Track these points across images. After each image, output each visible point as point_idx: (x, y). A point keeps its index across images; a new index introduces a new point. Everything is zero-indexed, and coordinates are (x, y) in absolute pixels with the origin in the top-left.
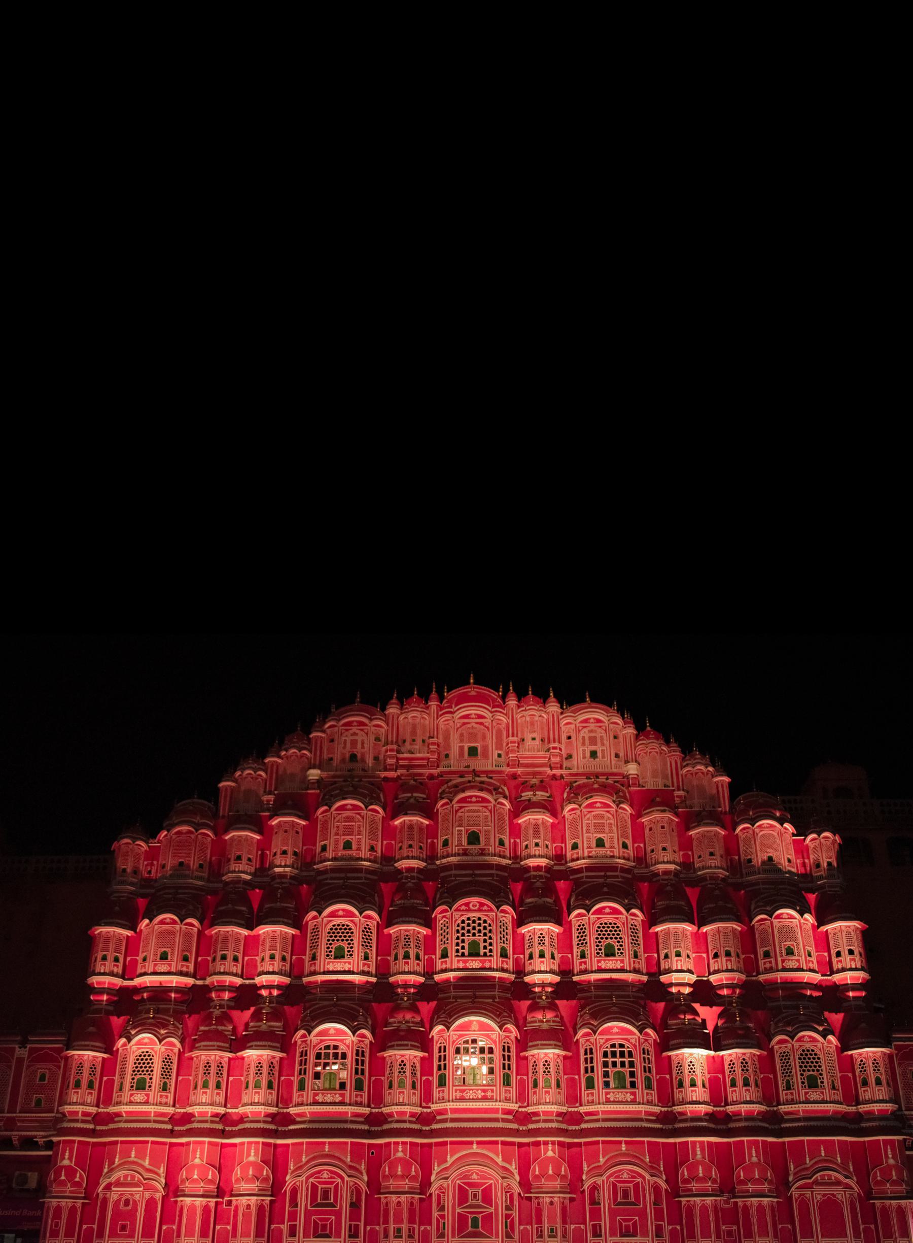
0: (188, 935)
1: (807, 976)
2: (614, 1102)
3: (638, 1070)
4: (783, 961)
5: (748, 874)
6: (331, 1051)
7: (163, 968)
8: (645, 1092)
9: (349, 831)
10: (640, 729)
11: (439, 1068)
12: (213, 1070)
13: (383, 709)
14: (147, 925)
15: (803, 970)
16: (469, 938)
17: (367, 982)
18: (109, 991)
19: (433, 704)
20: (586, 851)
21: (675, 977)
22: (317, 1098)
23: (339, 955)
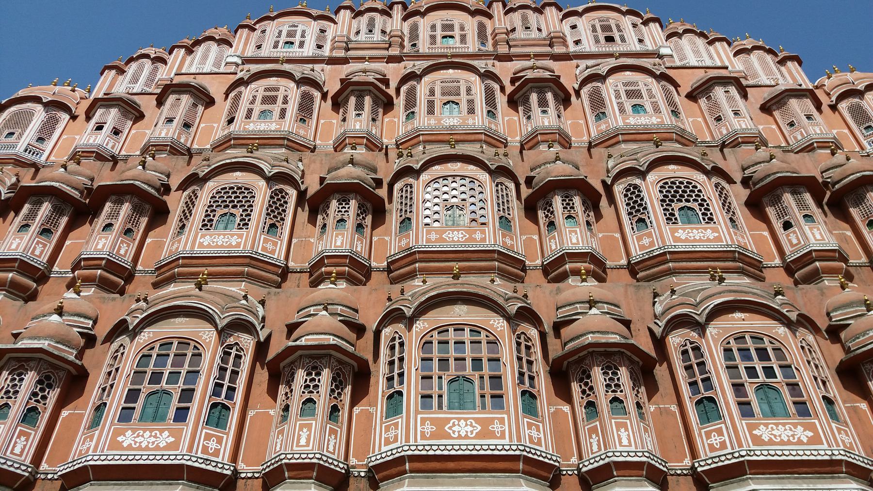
2: (771, 442)
8: (833, 425)
11: (390, 379)
20: (619, 119)
22: (120, 439)
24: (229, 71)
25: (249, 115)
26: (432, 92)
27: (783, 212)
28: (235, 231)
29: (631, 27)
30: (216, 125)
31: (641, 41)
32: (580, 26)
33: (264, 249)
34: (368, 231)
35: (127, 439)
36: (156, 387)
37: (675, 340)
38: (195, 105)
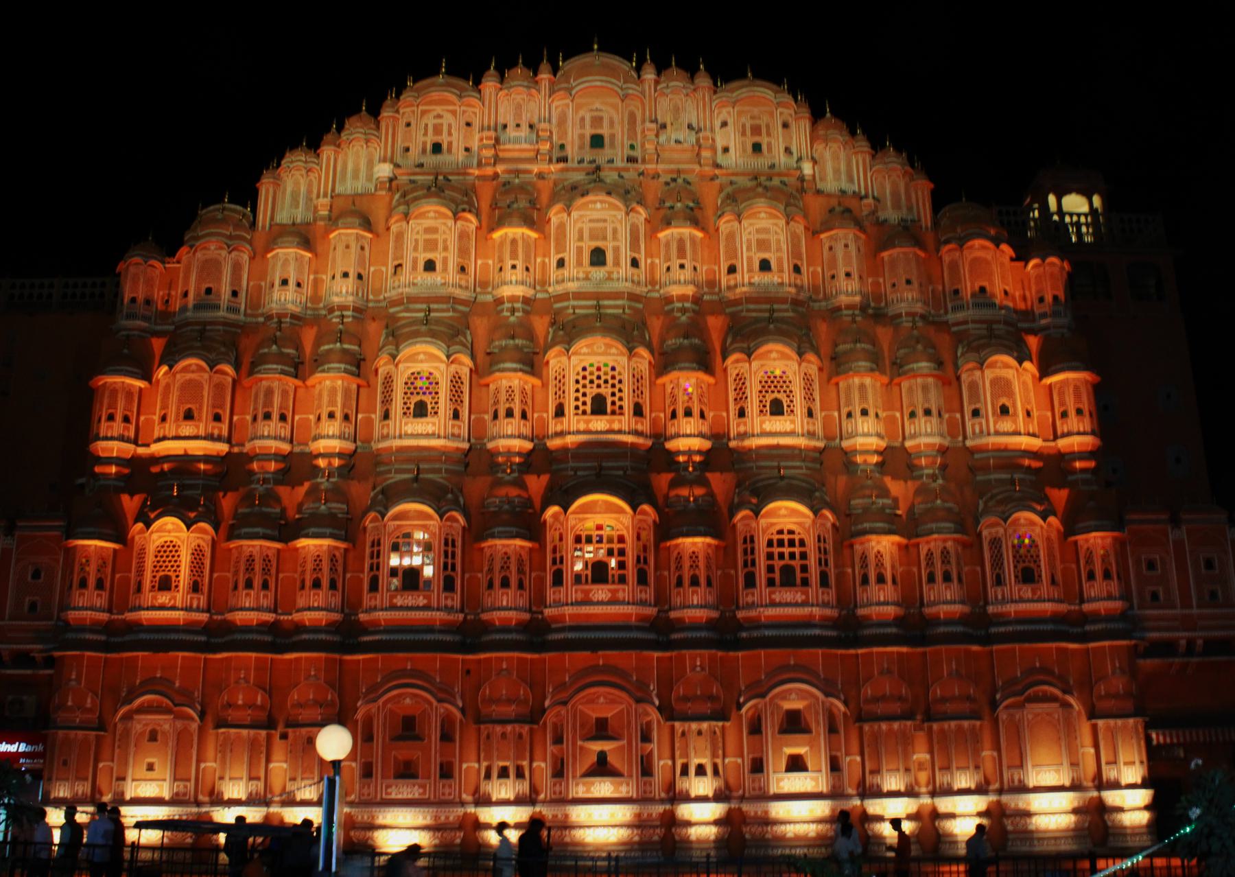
0: (219, 388)
1: (1024, 442)
3: (812, 562)
4: (995, 423)
5: (954, 309)
7: (188, 429)
9: (431, 245)
10: (817, 116)
12: (258, 567)
13: (477, 83)
14: (165, 374)
15: (1020, 434)
16: (592, 391)
17: (457, 449)
18: (118, 461)
19: (545, 76)
21: (860, 441)
23: (421, 411)
25: (414, 268)
26: (581, 238)
27: (849, 403)
28: (429, 419)
30: (384, 269)
32: (730, 121)
38: (362, 248)
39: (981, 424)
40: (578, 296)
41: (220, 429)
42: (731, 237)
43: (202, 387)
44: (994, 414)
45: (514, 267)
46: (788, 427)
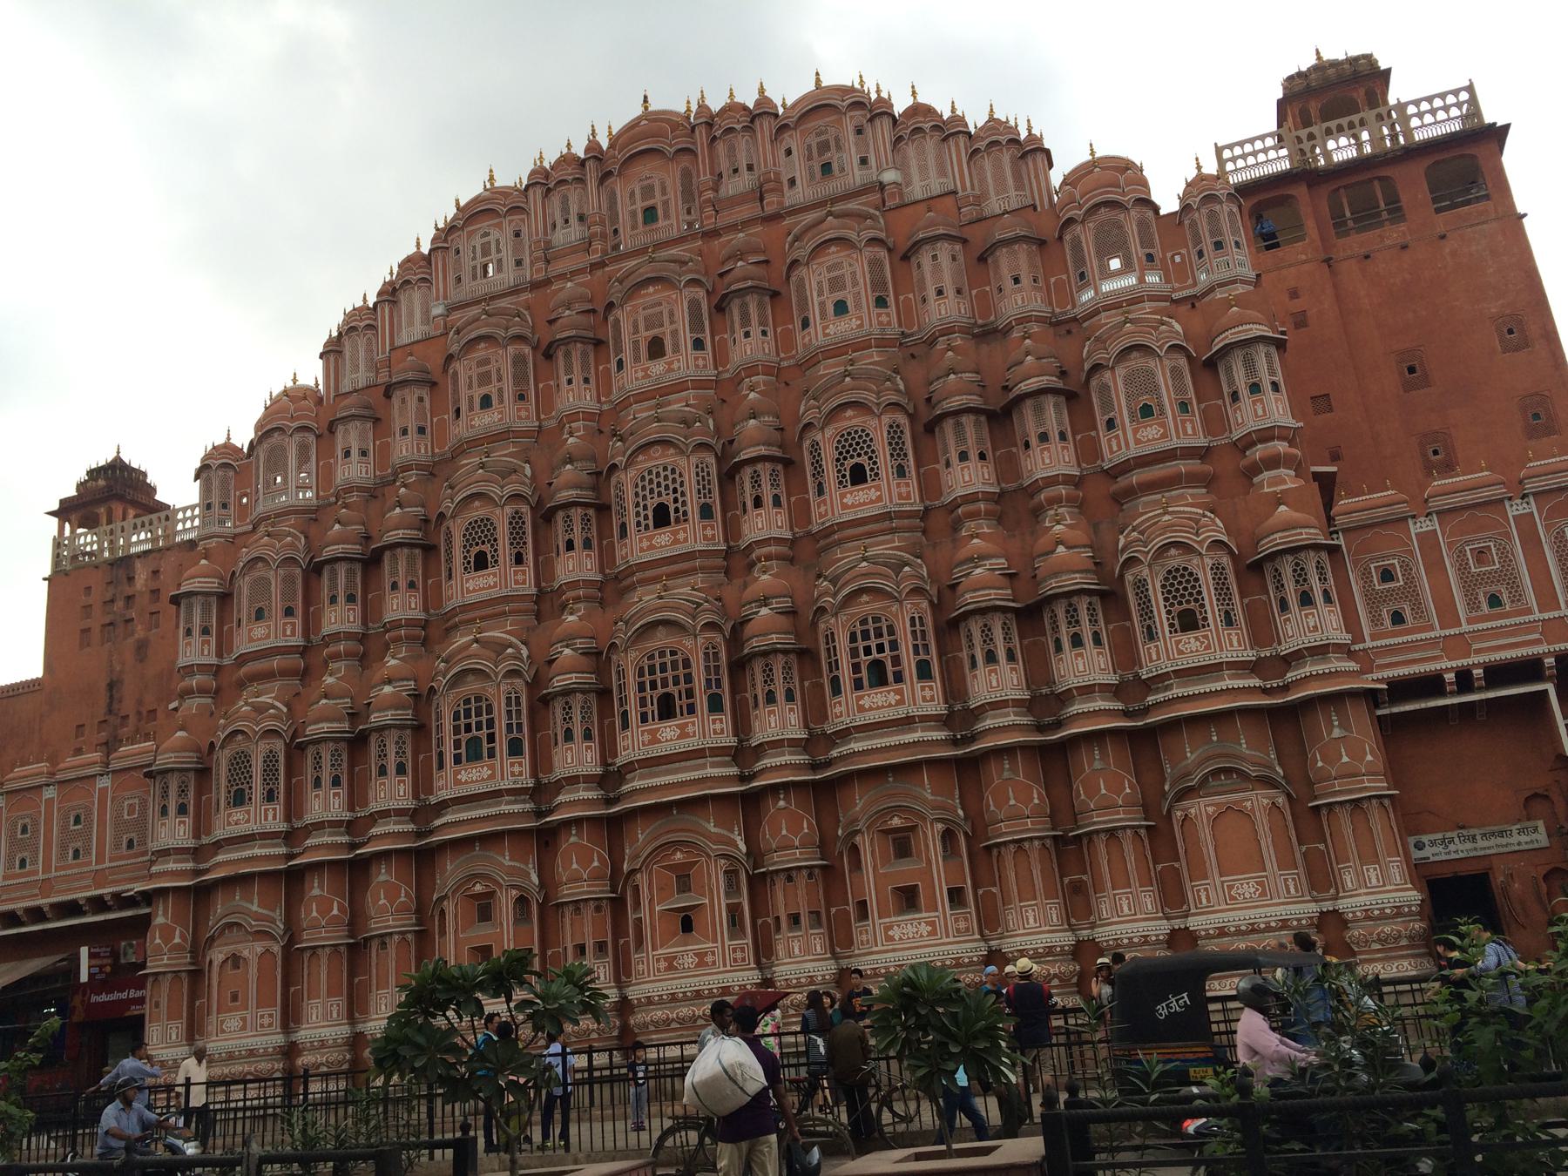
2: (871, 709)
4: (1135, 431)
6: (473, 705)
7: (259, 631)
8: (918, 686)
16: (652, 503)
23: (481, 563)
24: (438, 333)
25: (471, 409)
26: (636, 331)
27: (946, 451)
28: (490, 570)
29: (852, 138)
31: (864, 161)
33: (517, 582)
34: (595, 543)
35: (463, 777)
36: (469, 735)
37: (822, 626)
38: (421, 399)
39: (1117, 437)
40: (641, 397)
41: (293, 625)
42: (801, 285)
43: (267, 582)
44: (1133, 418)
45: (570, 382)
46: (873, 494)
